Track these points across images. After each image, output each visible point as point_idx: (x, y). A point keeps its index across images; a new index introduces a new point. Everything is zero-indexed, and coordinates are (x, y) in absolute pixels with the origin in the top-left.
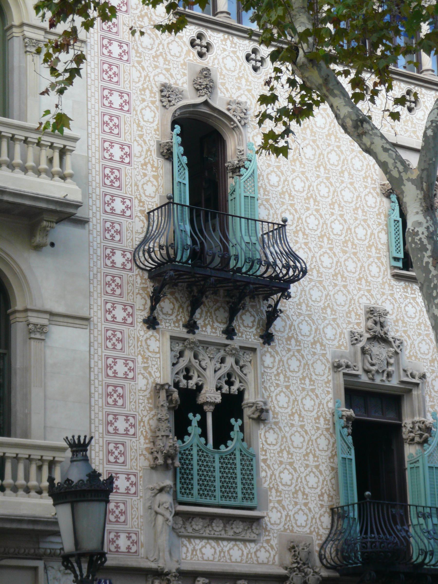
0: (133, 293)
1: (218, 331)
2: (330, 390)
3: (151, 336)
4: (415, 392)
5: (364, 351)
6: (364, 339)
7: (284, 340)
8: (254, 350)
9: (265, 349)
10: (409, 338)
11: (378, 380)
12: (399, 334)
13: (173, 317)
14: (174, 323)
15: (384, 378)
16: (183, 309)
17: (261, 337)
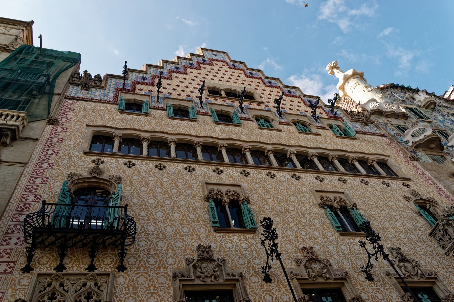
0: (18, 256)
1: (82, 269)
2: (170, 291)
3: (25, 277)
4: (238, 285)
5: (195, 267)
6: (196, 261)
7: (135, 269)
8: (108, 275)
9: (120, 274)
10: (230, 258)
11: (208, 281)
12: (222, 257)
13: (48, 265)
14: (47, 268)
15: (213, 279)
16: (56, 261)
17: (117, 268)
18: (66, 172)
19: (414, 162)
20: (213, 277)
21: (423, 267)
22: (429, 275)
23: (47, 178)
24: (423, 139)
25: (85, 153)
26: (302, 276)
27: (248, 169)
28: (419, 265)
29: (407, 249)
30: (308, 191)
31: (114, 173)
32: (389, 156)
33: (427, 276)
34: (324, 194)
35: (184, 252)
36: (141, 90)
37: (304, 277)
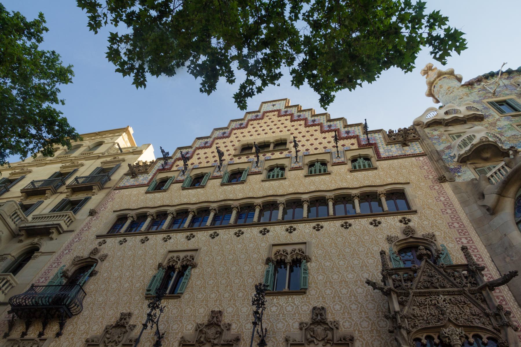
18: (75, 254)
19: (442, 184)
20: (115, 343)
21: (343, 329)
22: (341, 340)
23: (61, 263)
24: (470, 150)
25: (98, 237)
26: (189, 342)
27: (220, 230)
28: (337, 328)
29: (337, 307)
30: (266, 247)
31: (106, 252)
32: (409, 183)
33: (335, 342)
34: (281, 248)
35: (110, 319)
36: (177, 166)
37: (191, 343)
